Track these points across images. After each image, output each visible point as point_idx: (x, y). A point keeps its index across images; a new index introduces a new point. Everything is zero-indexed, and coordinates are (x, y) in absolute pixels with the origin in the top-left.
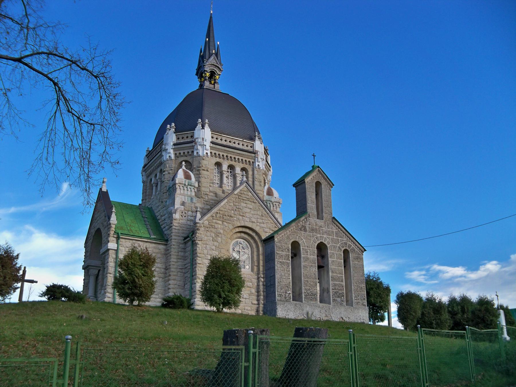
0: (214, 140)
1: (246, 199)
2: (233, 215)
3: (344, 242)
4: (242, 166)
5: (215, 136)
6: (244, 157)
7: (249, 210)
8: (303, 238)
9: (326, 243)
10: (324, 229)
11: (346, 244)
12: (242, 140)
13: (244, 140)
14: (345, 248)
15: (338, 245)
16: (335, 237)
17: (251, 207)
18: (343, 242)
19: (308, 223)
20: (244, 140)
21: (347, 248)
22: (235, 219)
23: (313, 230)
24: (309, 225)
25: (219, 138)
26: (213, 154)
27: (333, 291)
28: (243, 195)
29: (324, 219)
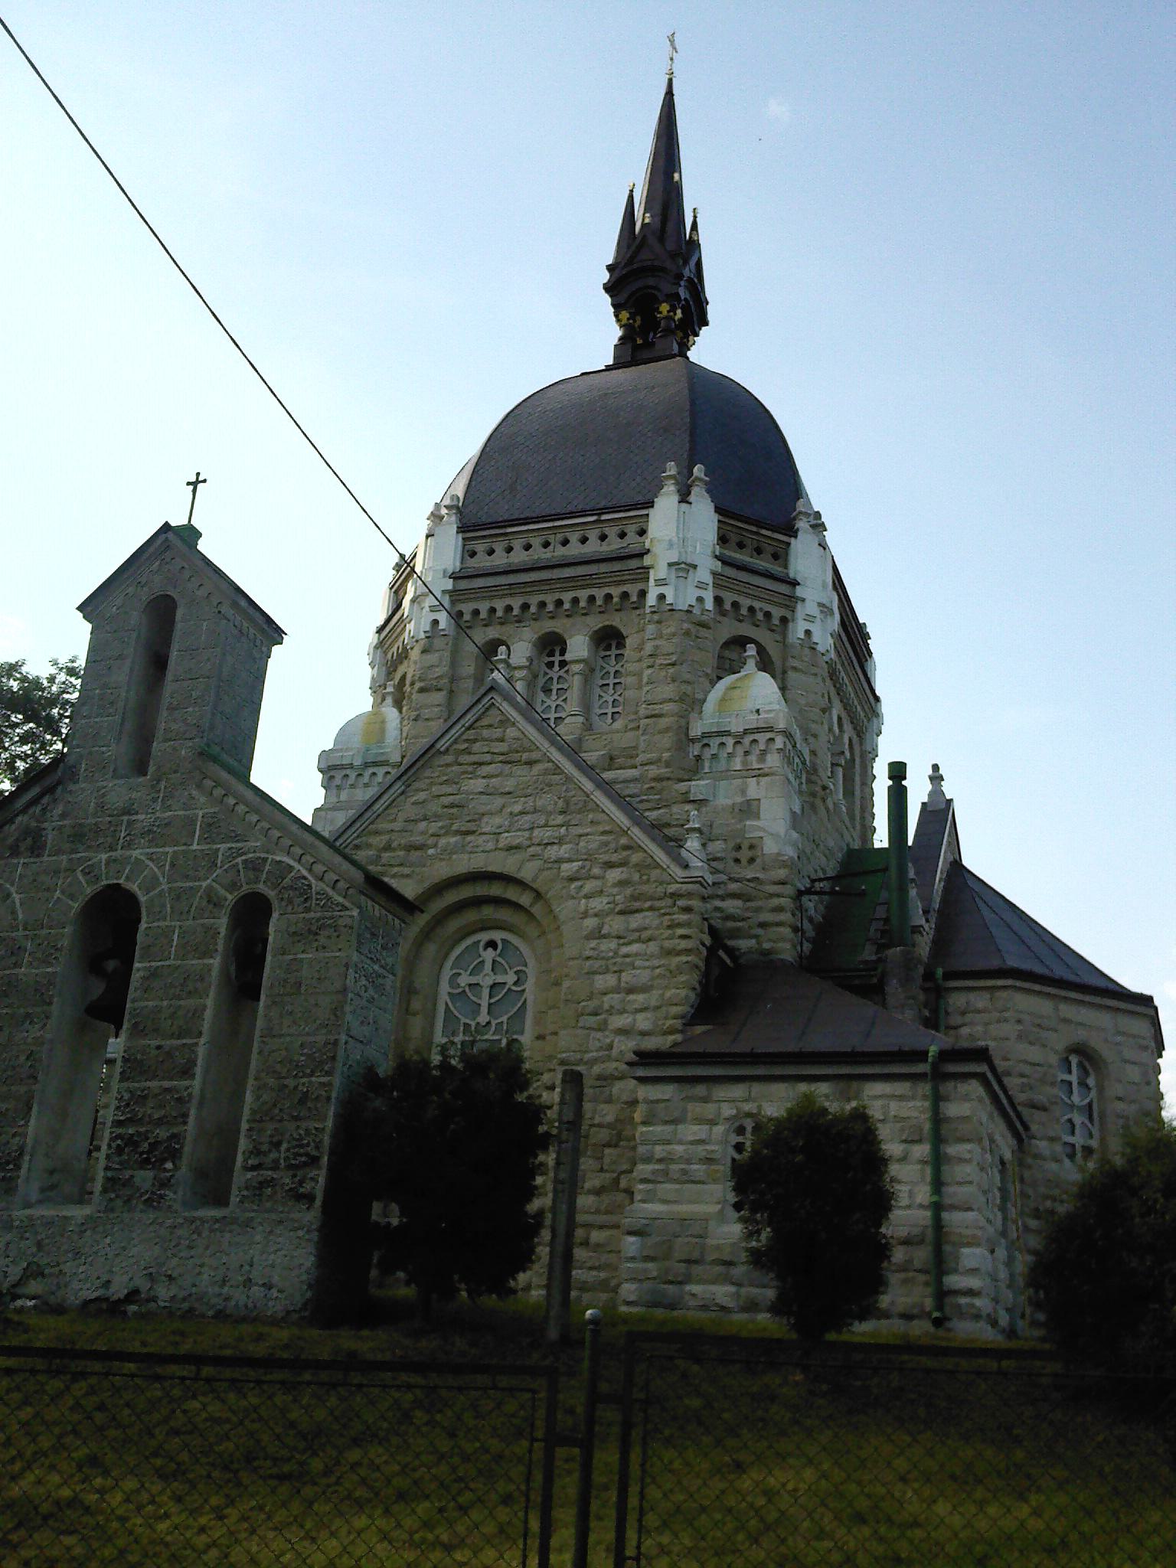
0: (482, 562)
1: (488, 758)
2: (418, 839)
3: (245, 862)
4: (596, 622)
5: (480, 547)
6: (600, 586)
7: (499, 801)
8: (13, 890)
9: (134, 887)
10: (143, 816)
11: (255, 866)
12: (594, 518)
13: (604, 517)
14: (245, 889)
15: (204, 884)
16: (195, 847)
17: (509, 784)
18: (239, 860)
19: (59, 810)
20: (604, 517)
21: (261, 887)
22: (431, 851)
23: (78, 836)
24: (63, 816)
25: (499, 547)
26: (727, 606)
27: (120, 1131)
28: (476, 747)
29: (151, 769)
